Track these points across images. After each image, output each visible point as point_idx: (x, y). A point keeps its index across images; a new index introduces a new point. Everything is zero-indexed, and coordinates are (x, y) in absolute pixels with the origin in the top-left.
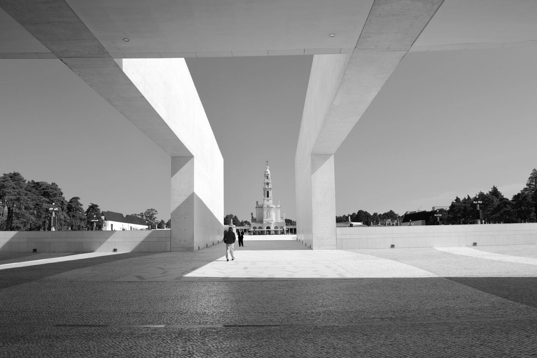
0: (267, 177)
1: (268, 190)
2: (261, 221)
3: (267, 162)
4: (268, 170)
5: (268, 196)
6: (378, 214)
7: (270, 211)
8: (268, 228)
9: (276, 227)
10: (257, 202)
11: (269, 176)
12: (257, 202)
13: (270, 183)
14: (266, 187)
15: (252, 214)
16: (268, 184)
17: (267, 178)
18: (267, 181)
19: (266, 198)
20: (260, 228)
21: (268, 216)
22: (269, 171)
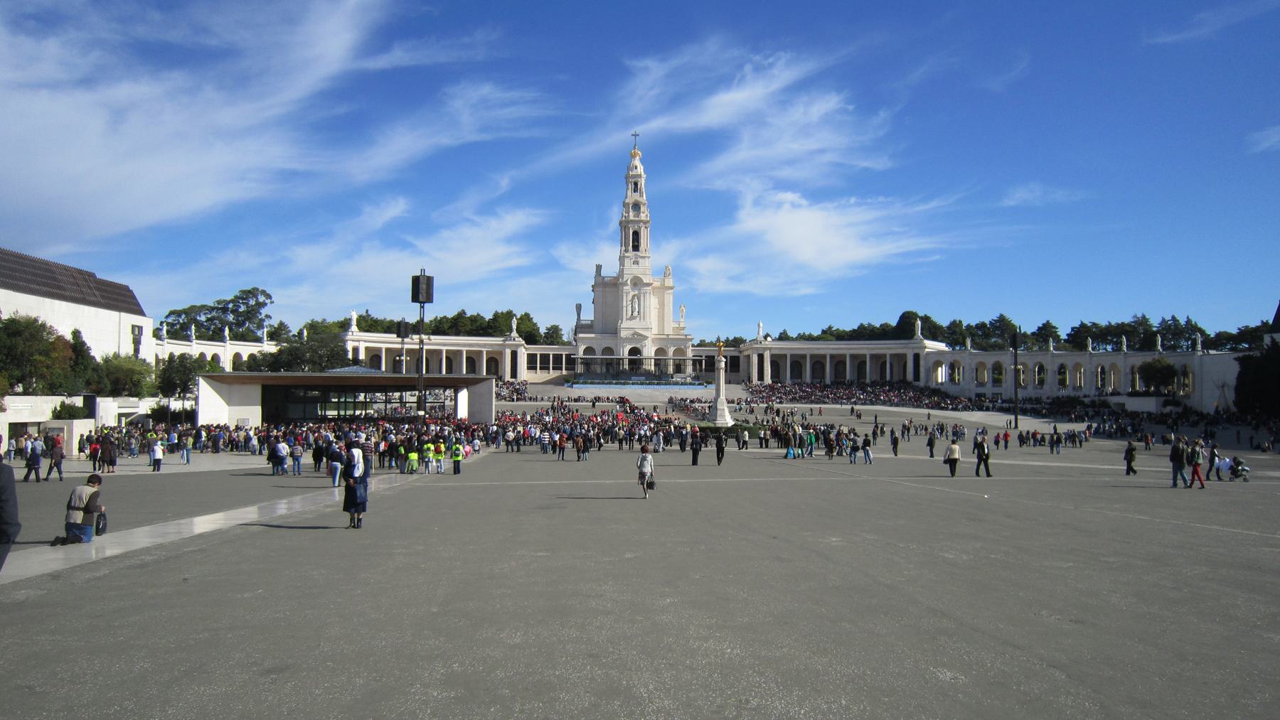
0: (636, 184)
2: (615, 332)
4: (637, 162)
5: (636, 248)
6: (965, 324)
7: (642, 298)
9: (659, 351)
10: (599, 268)
11: (642, 183)
12: (599, 268)
13: (644, 204)
14: (632, 216)
15: (579, 308)
16: (636, 206)
17: (635, 191)
18: (632, 197)
19: (631, 254)
20: (608, 350)
21: (636, 314)
22: (642, 167)
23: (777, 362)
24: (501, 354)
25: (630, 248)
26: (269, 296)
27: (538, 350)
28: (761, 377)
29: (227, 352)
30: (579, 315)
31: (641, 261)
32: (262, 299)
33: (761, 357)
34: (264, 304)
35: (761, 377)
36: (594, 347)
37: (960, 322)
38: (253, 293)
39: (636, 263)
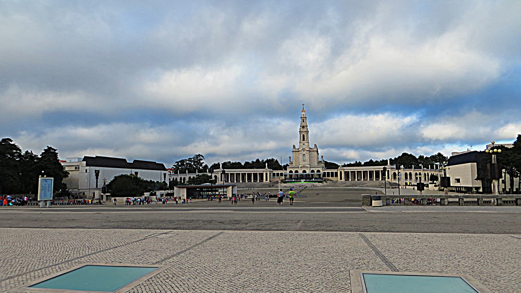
0: (303, 120)
1: (304, 134)
3: (303, 105)
5: (304, 140)
8: (304, 171)
21: (304, 160)
23: (347, 174)
24: (263, 173)
25: (302, 139)
26: (203, 157)
27: (276, 172)
28: (341, 179)
29: (187, 176)
30: (290, 160)
31: (305, 144)
32: (201, 158)
33: (341, 172)
34: (202, 159)
35: (341, 179)
36: (292, 170)
37: (423, 156)
38: (199, 155)
39: (304, 144)
